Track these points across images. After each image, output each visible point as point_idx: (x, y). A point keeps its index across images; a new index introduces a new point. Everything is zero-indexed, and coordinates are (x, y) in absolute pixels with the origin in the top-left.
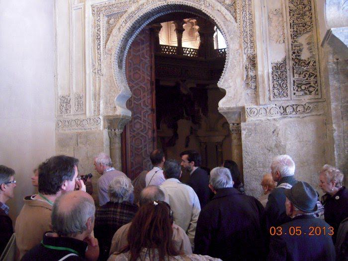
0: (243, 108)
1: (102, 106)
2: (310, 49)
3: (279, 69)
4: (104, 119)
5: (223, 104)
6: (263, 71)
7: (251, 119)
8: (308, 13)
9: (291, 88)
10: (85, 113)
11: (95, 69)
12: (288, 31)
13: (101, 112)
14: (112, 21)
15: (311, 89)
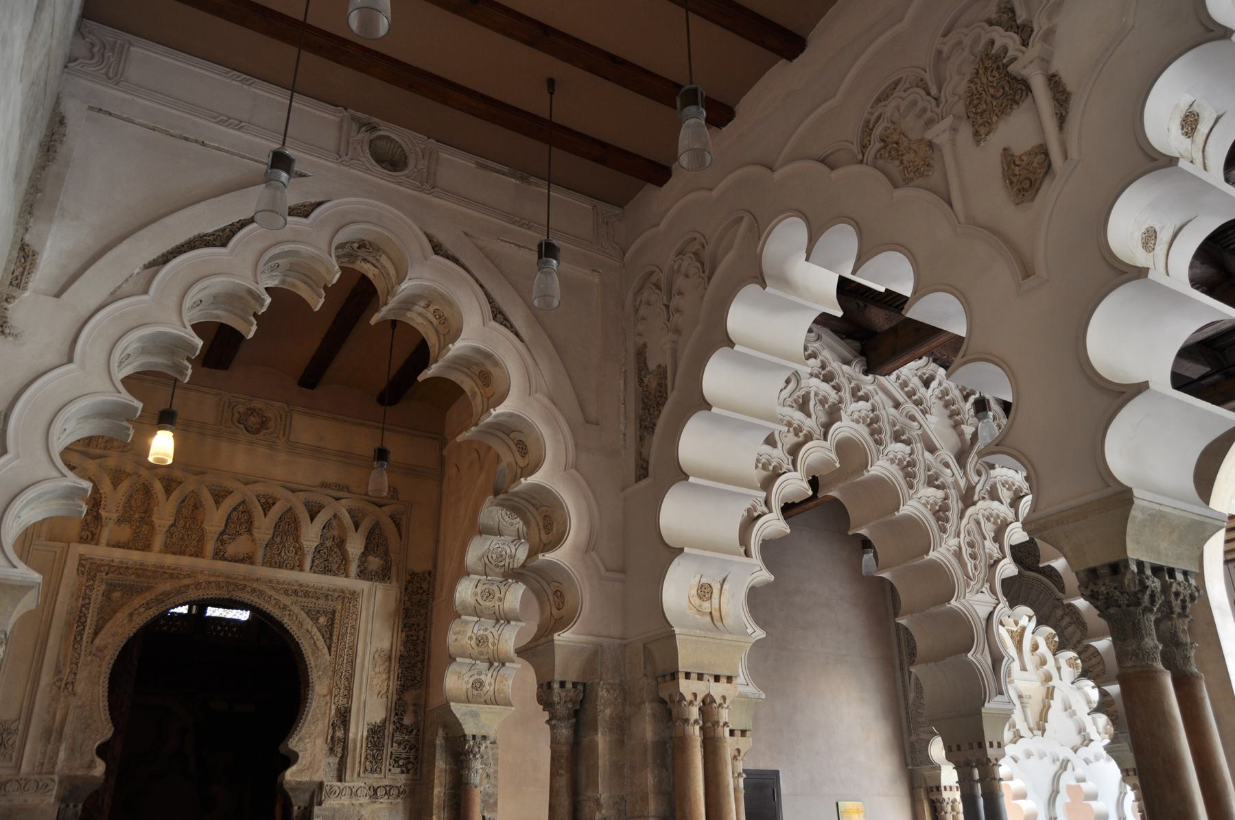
0: (321, 784)
1: (62, 755)
2: (415, 712)
3: (375, 733)
4: (61, 782)
5: (291, 775)
6: (356, 734)
7: (331, 803)
8: (419, 665)
9: (386, 762)
10: (18, 767)
11: (61, 680)
12: (394, 685)
13: (58, 767)
14: (116, 595)
15: (410, 766)
